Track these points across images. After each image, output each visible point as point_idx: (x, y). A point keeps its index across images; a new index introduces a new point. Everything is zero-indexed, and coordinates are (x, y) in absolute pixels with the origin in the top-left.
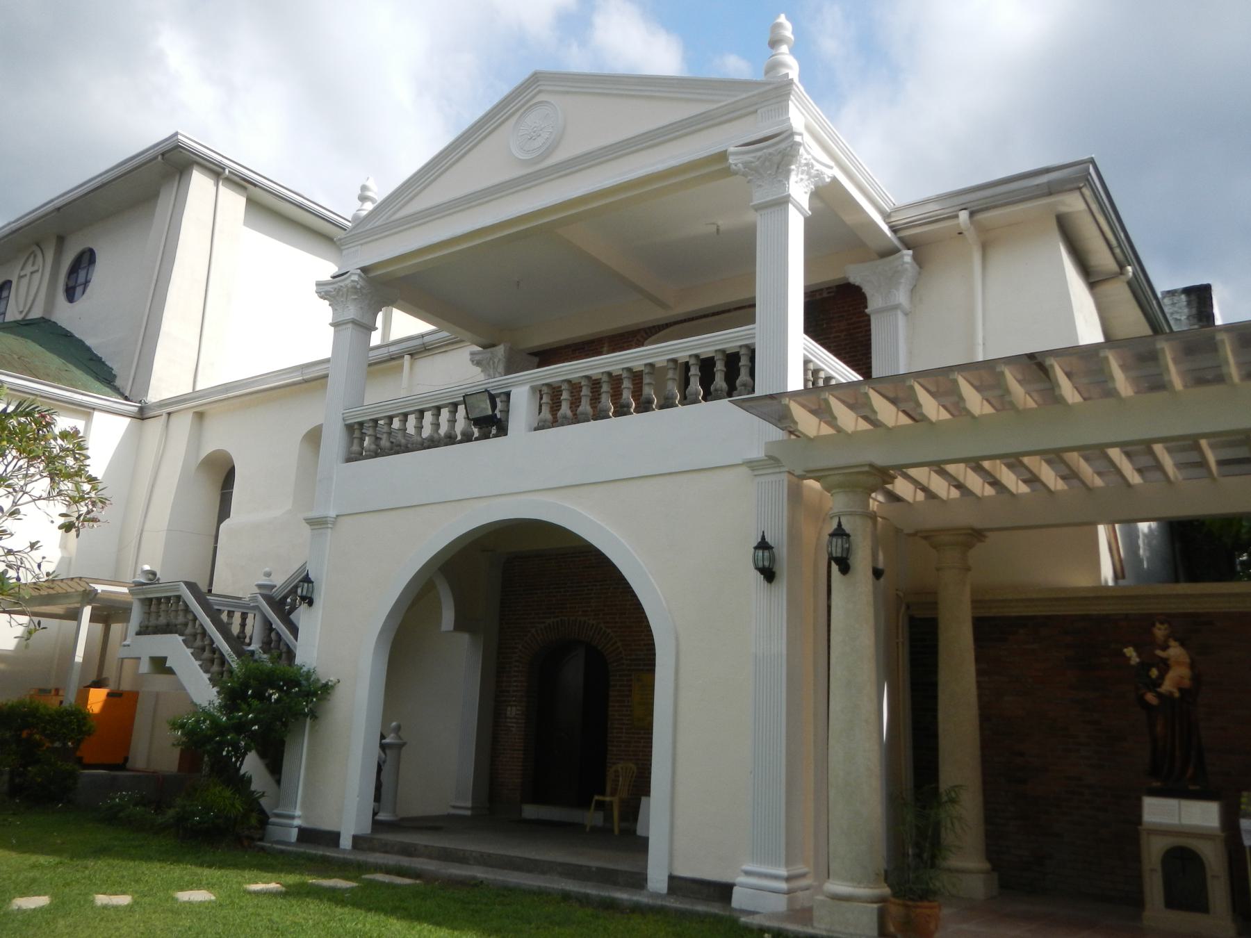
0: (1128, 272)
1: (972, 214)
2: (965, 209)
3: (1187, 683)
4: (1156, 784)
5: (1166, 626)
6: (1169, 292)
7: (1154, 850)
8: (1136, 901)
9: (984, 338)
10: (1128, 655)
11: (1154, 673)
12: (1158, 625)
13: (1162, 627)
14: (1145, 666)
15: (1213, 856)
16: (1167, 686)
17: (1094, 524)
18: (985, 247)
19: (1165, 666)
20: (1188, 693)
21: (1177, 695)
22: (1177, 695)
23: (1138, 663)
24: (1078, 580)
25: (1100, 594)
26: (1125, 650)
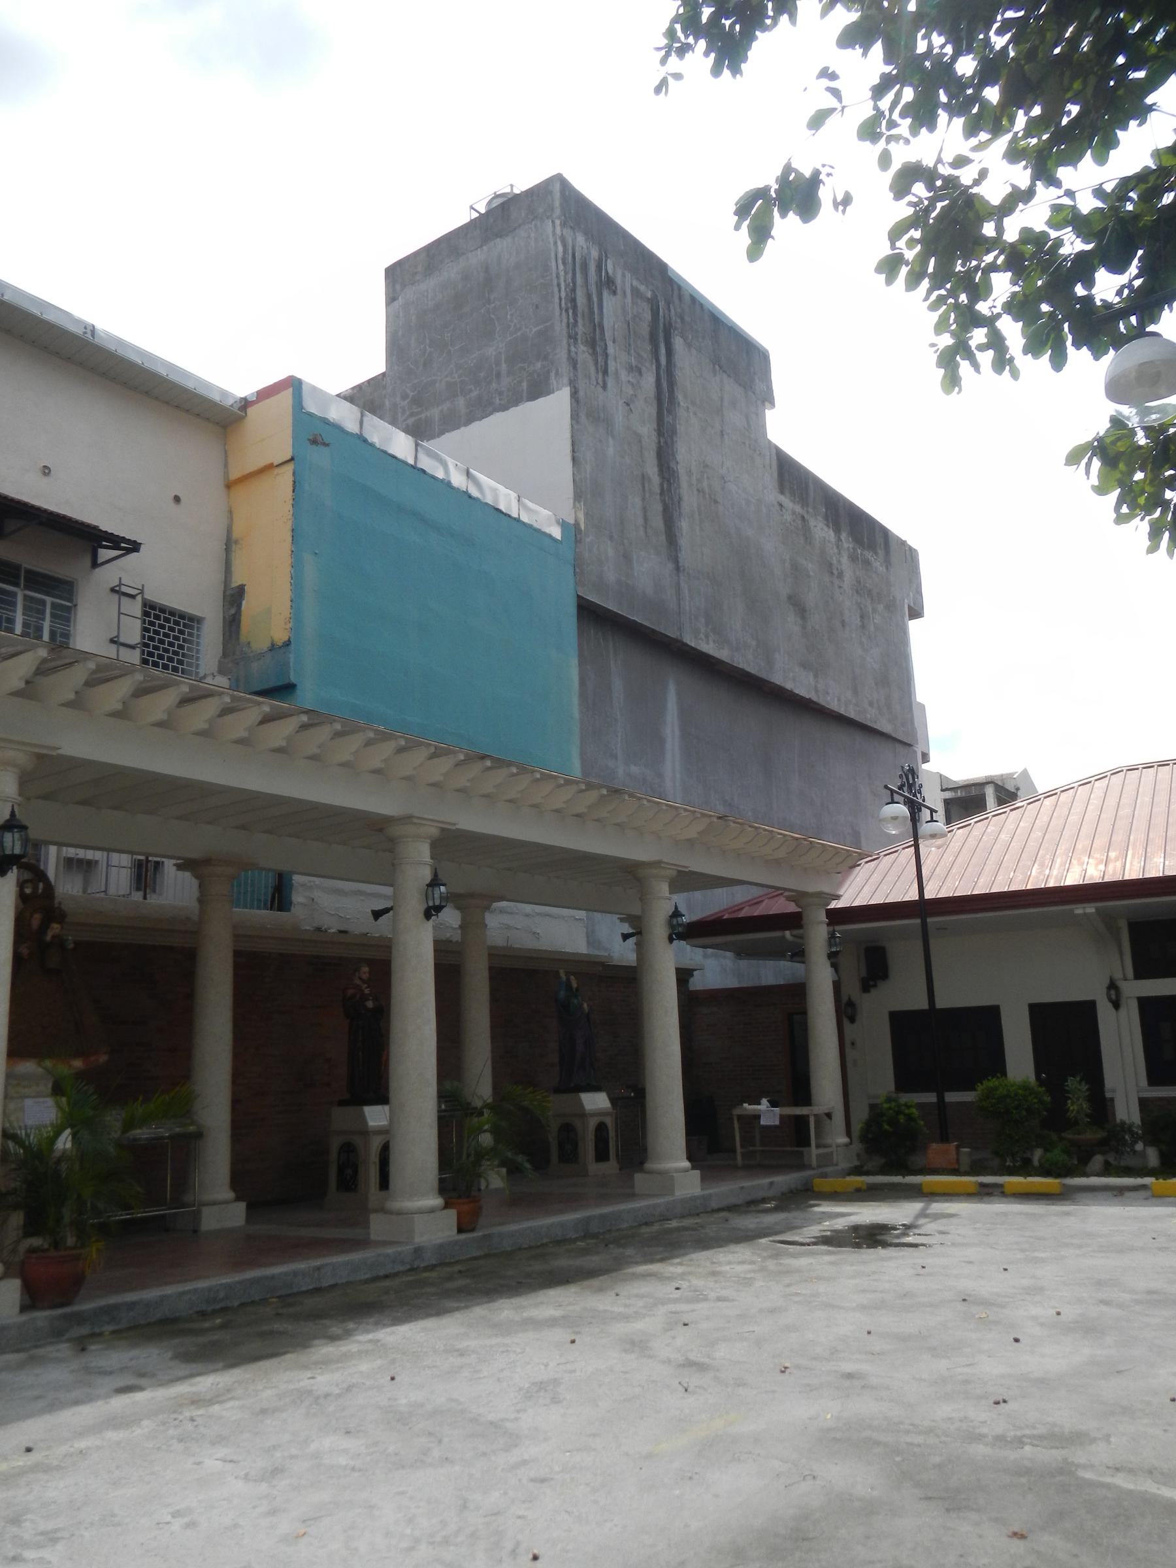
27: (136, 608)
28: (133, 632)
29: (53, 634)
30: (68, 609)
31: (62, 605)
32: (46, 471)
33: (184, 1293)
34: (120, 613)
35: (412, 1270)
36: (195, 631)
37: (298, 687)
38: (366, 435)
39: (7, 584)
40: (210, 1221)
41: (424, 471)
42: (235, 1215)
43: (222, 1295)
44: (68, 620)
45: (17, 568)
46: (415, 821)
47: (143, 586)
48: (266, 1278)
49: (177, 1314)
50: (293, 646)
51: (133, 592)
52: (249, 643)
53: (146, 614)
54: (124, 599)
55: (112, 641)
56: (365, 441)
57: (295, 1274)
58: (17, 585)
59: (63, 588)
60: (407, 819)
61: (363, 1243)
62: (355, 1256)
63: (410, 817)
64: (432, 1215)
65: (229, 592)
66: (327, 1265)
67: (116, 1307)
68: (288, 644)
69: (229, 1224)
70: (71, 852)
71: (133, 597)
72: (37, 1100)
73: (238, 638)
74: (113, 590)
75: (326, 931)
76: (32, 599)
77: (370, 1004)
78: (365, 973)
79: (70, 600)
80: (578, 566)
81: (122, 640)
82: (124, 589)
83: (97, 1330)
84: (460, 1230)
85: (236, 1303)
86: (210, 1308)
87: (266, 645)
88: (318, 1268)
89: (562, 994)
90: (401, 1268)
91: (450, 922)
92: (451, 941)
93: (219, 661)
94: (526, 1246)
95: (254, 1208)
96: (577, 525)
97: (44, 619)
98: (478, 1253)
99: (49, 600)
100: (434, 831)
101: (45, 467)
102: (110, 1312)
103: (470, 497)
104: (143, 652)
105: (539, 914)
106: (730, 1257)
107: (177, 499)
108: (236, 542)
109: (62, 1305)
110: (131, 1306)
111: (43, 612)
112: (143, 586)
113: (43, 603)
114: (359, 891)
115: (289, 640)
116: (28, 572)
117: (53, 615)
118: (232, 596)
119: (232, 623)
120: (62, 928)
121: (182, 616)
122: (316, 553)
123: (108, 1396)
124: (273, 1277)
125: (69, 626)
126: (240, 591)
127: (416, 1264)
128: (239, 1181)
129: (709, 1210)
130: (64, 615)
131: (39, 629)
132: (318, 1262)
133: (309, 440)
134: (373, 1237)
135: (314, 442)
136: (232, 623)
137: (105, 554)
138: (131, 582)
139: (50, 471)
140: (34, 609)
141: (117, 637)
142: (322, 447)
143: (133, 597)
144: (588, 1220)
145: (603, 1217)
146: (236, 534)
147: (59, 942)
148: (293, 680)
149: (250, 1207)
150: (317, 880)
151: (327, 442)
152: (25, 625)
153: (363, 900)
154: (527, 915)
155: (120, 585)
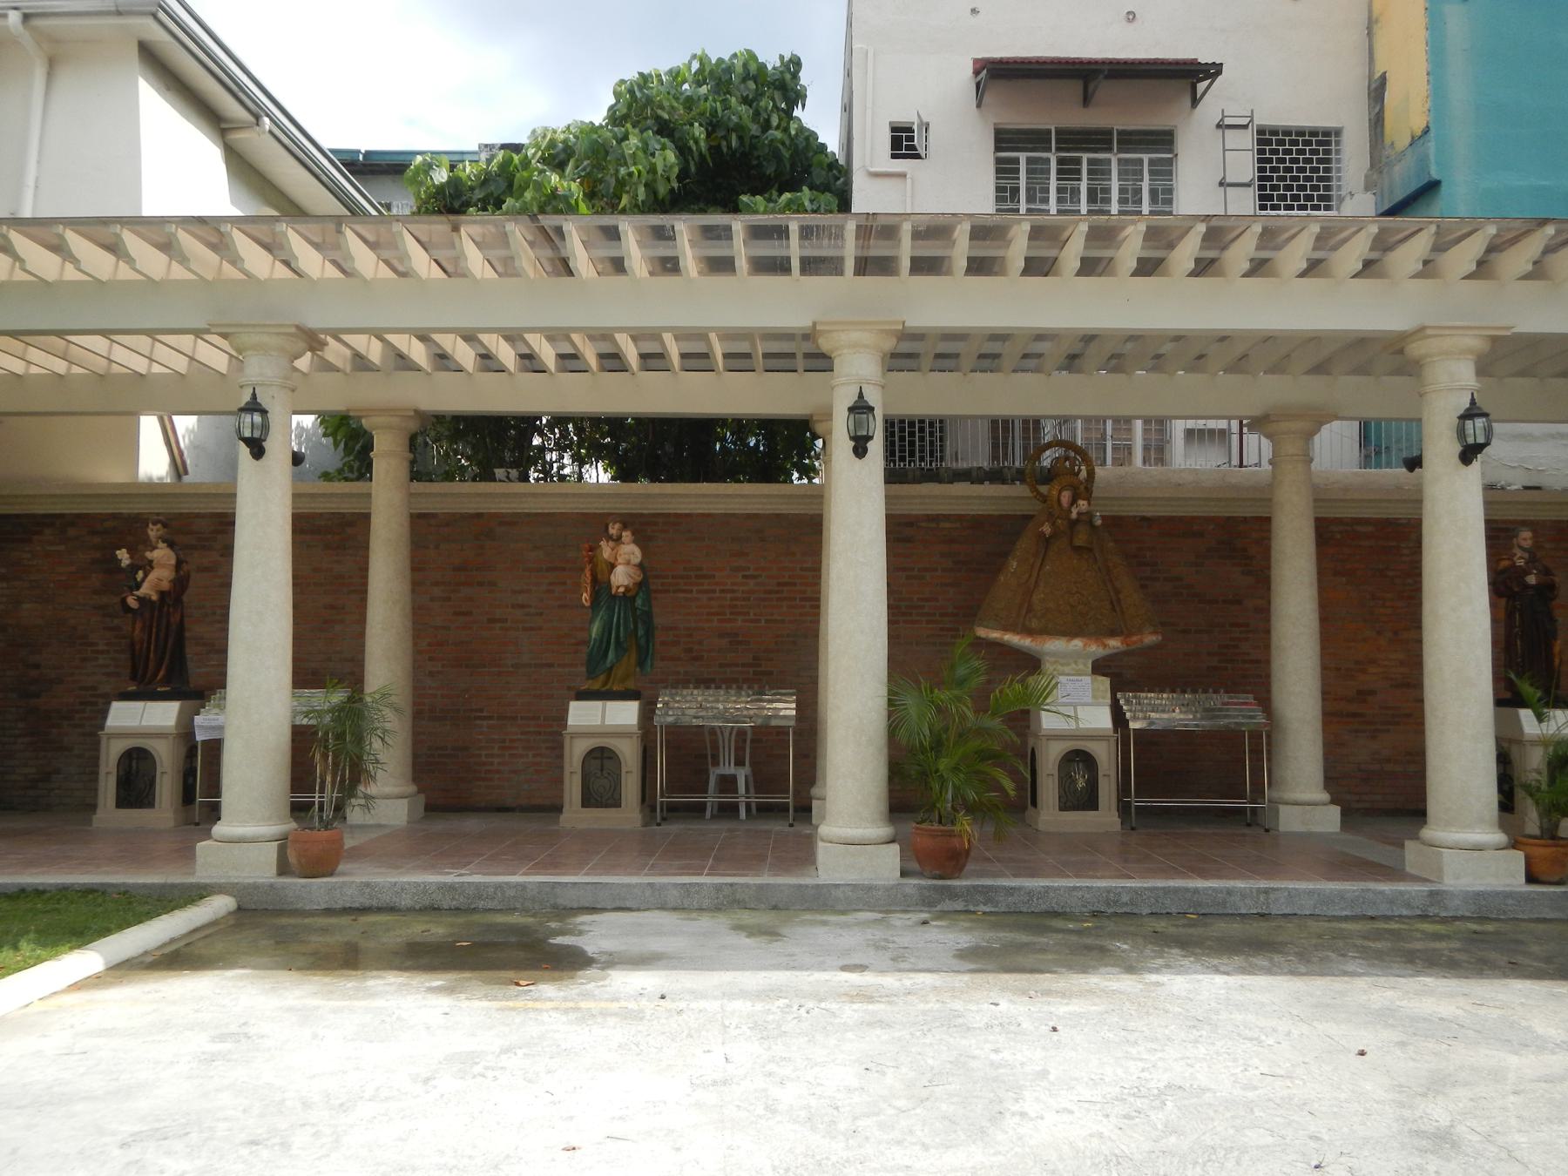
0: (264, 124)
1: (26, 17)
2: (16, 8)
3: (165, 586)
4: (132, 688)
5: (159, 526)
6: (486, 146)
7: (112, 753)
8: (93, 807)
9: (37, 179)
10: (119, 557)
11: (140, 574)
12: (151, 526)
13: (155, 528)
14: (134, 568)
15: (166, 758)
16: (145, 590)
17: (134, 415)
18: (52, 64)
19: (149, 566)
20: (174, 596)
21: (155, 597)
22: (155, 597)
23: (128, 565)
24: (110, 474)
25: (152, 490)
26: (118, 552)
27: (1247, 140)
28: (1244, 166)
29: (1154, 194)
30: (1170, 162)
31: (1163, 159)
32: (1131, 17)
33: (1075, 888)
34: (1224, 150)
36: (1333, 147)
37: (1443, 184)
39: (1096, 152)
40: (1290, 820)
42: (1329, 819)
43: (1125, 898)
44: (1170, 173)
45: (1109, 132)
46: (1429, 332)
47: (1252, 111)
48: (1187, 890)
49: (1068, 910)
50: (1432, 134)
51: (1244, 121)
52: (1392, 144)
53: (1260, 142)
54: (1228, 132)
55: (1221, 184)
57: (1229, 892)
58: (1110, 150)
59: (1163, 140)
60: (1420, 332)
61: (1394, 872)
62: (1386, 887)
63: (1422, 329)
64: (1476, 853)
65: (1373, 86)
66: (1277, 889)
67: (990, 888)
68: (1426, 131)
70: (1191, 424)
71: (1245, 127)
73: (1383, 141)
74: (1219, 126)
75: (1503, 488)
76: (1127, 161)
77: (1531, 580)
78: (1525, 539)
79: (1170, 151)
81: (1228, 180)
82: (1228, 121)
83: (972, 908)
84: (1531, 878)
85: (1146, 911)
87: (1407, 141)
88: (1266, 891)
90: (1405, 912)
93: (1366, 176)
95: (1350, 816)
97: (1142, 180)
99: (1146, 157)
100: (1475, 343)
101: (1129, 13)
102: (988, 894)
104: (1262, 188)
108: (1377, 21)
109: (941, 878)
110: (1010, 891)
112: (1252, 111)
113: (1141, 161)
114: (1558, 433)
115: (1427, 127)
116: (1120, 133)
117: (1151, 172)
118: (1376, 89)
119: (1377, 123)
120: (1089, 504)
121: (1314, 133)
123: (832, 968)
124: (1196, 891)
125: (1171, 180)
126: (1383, 78)
127: (1432, 911)
128: (1335, 780)
130: (1164, 170)
131: (1138, 191)
132: (1263, 884)
134: (1408, 869)
136: (1377, 123)
137: (1201, 86)
138: (1236, 111)
139: (1134, 16)
140: (1130, 171)
141: (1224, 178)
143: (1245, 127)
146: (1376, 12)
147: (1087, 518)
148: (1435, 175)
149: (1343, 814)
152: (1122, 191)
155: (1224, 117)
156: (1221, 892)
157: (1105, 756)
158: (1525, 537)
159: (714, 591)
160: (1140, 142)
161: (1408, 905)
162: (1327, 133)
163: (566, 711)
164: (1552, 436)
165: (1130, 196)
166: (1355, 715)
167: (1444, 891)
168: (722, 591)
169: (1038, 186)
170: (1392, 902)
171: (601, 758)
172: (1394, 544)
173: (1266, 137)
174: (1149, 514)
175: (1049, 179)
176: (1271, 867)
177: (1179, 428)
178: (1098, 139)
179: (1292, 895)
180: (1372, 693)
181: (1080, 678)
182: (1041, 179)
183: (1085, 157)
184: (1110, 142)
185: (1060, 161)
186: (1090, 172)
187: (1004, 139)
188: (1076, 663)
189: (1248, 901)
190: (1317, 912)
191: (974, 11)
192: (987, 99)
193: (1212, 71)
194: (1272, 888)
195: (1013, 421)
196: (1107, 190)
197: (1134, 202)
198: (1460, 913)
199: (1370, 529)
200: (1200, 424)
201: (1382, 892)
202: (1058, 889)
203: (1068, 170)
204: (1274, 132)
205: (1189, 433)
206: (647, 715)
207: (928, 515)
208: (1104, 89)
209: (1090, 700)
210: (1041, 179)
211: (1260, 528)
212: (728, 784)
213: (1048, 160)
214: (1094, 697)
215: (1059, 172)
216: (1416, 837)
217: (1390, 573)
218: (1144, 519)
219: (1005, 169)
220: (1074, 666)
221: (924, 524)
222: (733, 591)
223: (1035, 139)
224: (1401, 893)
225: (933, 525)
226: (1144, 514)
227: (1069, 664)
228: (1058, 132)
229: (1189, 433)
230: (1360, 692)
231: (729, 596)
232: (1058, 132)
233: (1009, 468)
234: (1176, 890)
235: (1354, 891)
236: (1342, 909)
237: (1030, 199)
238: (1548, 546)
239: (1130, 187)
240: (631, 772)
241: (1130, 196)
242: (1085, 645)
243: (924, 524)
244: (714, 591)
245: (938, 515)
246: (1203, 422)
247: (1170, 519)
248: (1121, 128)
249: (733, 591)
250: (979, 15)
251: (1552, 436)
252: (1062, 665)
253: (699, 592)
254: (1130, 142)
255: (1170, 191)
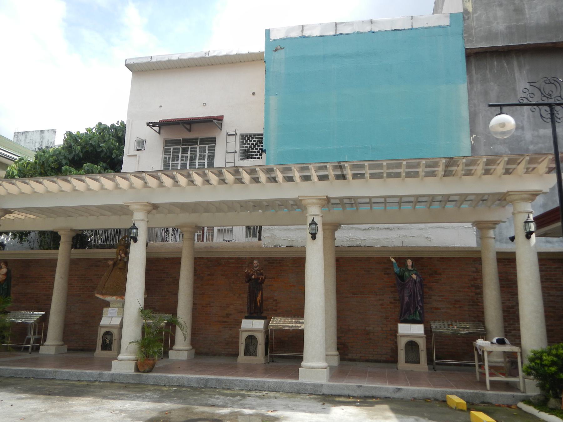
29: (209, 156)
30: (214, 147)
32: (205, 104)
33: (7, 369)
35: (79, 381)
38: (304, 35)
41: (341, 34)
43: (19, 373)
44: (214, 150)
48: (35, 371)
51: (234, 133)
56: (305, 37)
57: (46, 372)
59: (213, 140)
66: (59, 371)
69: (180, 358)
70: (219, 228)
72: (112, 308)
80: (467, 32)
86: (16, 376)
88: (56, 372)
89: (396, 269)
90: (92, 379)
91: (359, 237)
92: (360, 246)
94: (163, 384)
96: (466, 12)
98: (133, 382)
99: (207, 146)
103: (374, 33)
105: (432, 227)
106: (81, 402)
107: (254, 94)
111: (205, 150)
117: (209, 150)
122: (277, 94)
124: (38, 371)
127: (99, 379)
129: (321, 394)
130: (212, 149)
131: (204, 156)
133: (273, 51)
135: (276, 50)
138: (231, 130)
142: (281, 50)
144: (207, 380)
145: (218, 380)
150: (276, 227)
151: (283, 47)
153: (302, 232)
154: (421, 229)
156: (44, 371)
157: (261, 338)
158: (256, 263)
159: (45, 282)
160: (206, 141)
161: (93, 377)
162: (259, 135)
163: (241, 322)
164: (297, 229)
165: (202, 158)
166: (225, 322)
167: (103, 373)
168: (47, 282)
169: (176, 156)
170: (88, 376)
171: (251, 339)
172: (241, 265)
173: (243, 137)
174: (167, 257)
175: (179, 154)
176: (35, 362)
177: (216, 229)
178: (194, 141)
179: (62, 373)
180: (231, 314)
181: (114, 309)
182: (177, 154)
183: (190, 147)
184: (183, 142)
185: (183, 148)
186: (191, 151)
187: (167, 143)
188: (118, 304)
189: (51, 374)
190: (68, 378)
191: (160, 107)
192: (162, 131)
193: (220, 119)
194: (58, 371)
195: (99, 231)
196: (195, 156)
197: (203, 160)
198: (106, 380)
199: (233, 261)
200: (222, 228)
201: (86, 373)
202: (3, 369)
203: (185, 151)
204: (247, 135)
205: (219, 230)
206: (266, 325)
207: (104, 258)
208: (194, 126)
209: (116, 315)
210: (177, 154)
211: (176, 262)
212: (30, 339)
213: (179, 148)
214: (118, 314)
215: (182, 152)
216: (300, 367)
217: (238, 275)
218: (166, 258)
219: (166, 152)
220: (117, 305)
221: (103, 261)
222: (50, 282)
223: (176, 142)
224: (91, 373)
225: (105, 261)
226: (166, 257)
227: (115, 304)
228: (183, 140)
229: (219, 230)
230: (227, 314)
231: (48, 283)
232: (200, 138)
233: (99, 244)
234: (33, 371)
235: (79, 372)
236: (75, 378)
237: (173, 160)
238: (290, 265)
239: (202, 155)
240: (243, 343)
241: (202, 157)
242: (116, 298)
243: (103, 261)
244: (45, 282)
245: (107, 258)
246: (220, 227)
247: (173, 258)
248: (201, 137)
249: (50, 282)
250: (159, 107)
251: (297, 229)
252: (114, 304)
253: (41, 282)
254: (203, 141)
255: (214, 156)
